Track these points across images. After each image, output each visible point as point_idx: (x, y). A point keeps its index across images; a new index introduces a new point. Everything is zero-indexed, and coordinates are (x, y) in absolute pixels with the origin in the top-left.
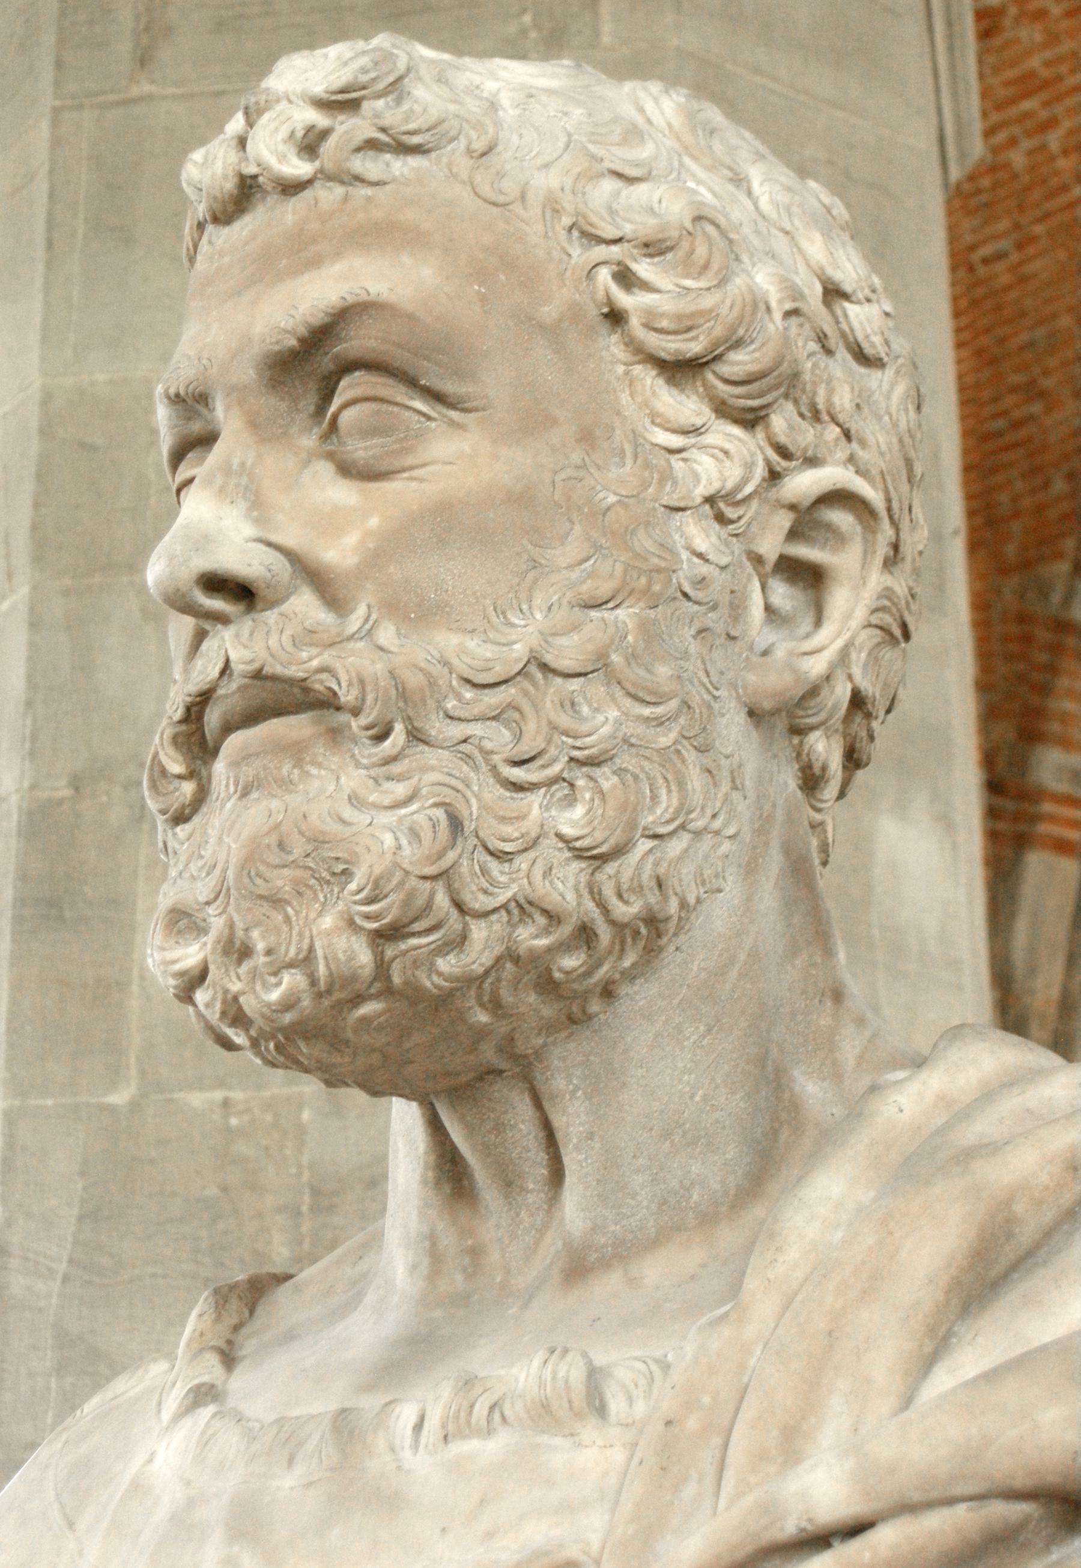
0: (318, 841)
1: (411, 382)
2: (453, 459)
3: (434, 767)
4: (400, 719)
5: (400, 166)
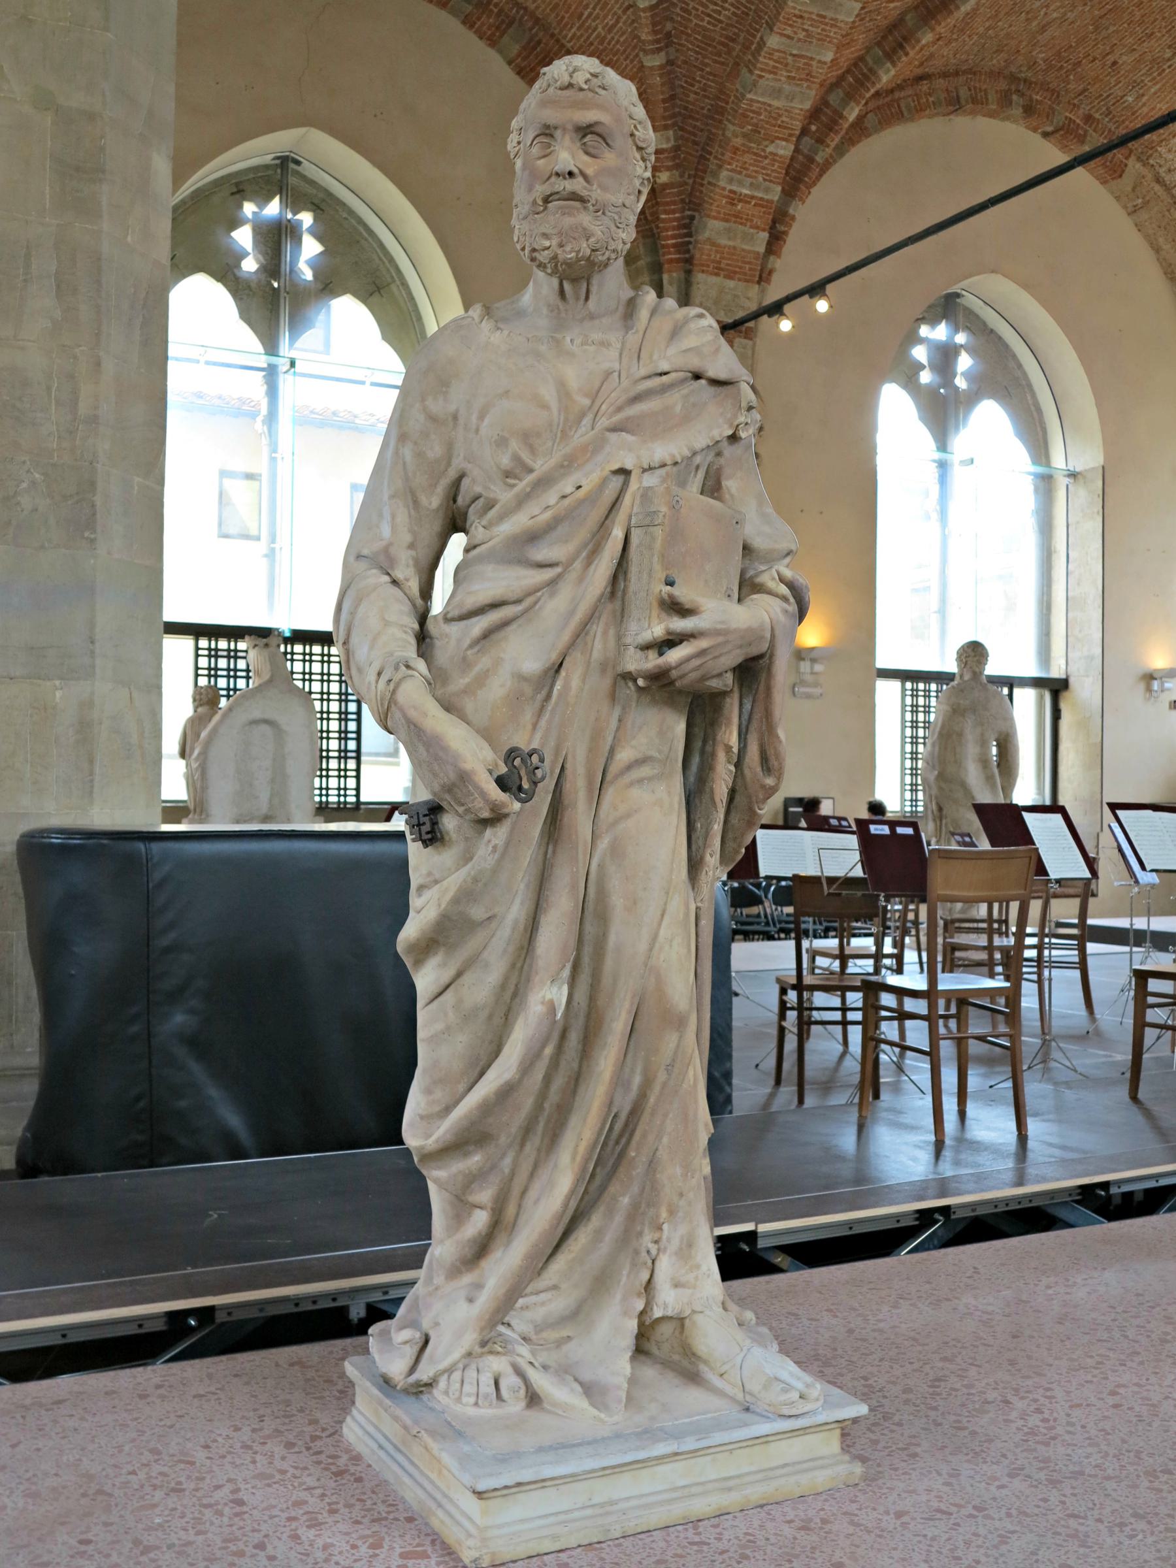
0: (585, 229)
1: (604, 139)
2: (610, 158)
3: (606, 221)
4: (600, 210)
5: (603, 92)
